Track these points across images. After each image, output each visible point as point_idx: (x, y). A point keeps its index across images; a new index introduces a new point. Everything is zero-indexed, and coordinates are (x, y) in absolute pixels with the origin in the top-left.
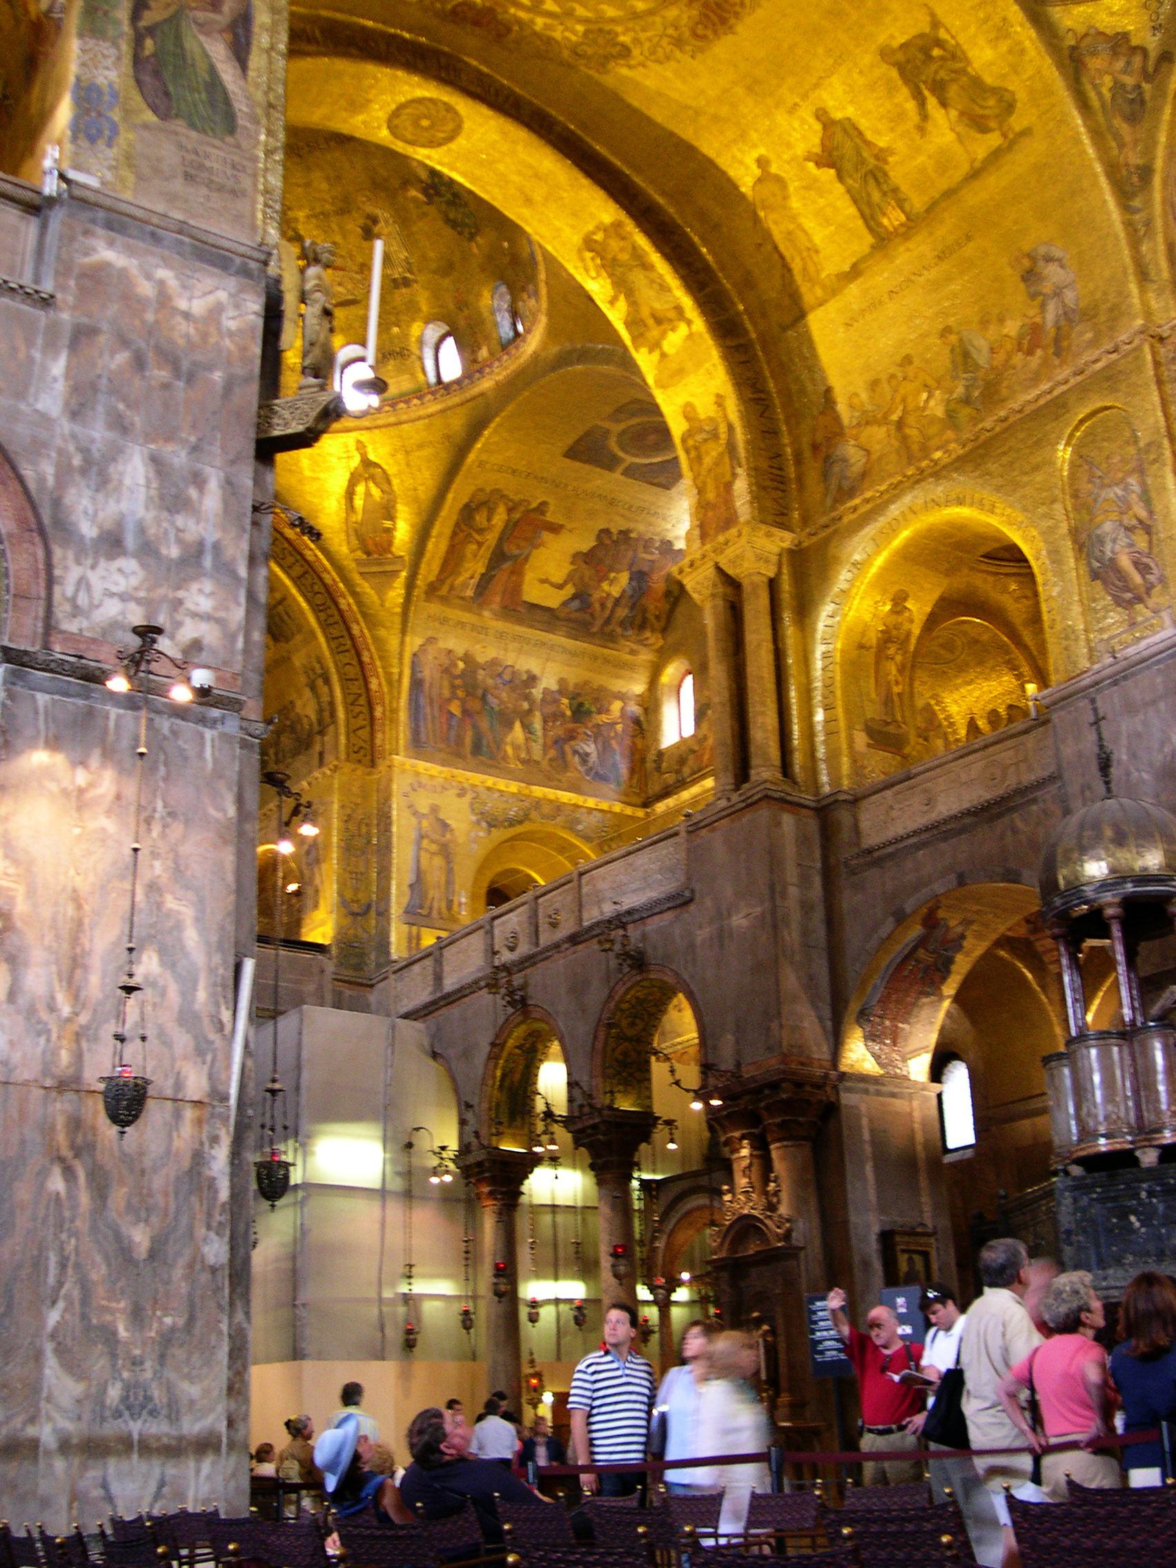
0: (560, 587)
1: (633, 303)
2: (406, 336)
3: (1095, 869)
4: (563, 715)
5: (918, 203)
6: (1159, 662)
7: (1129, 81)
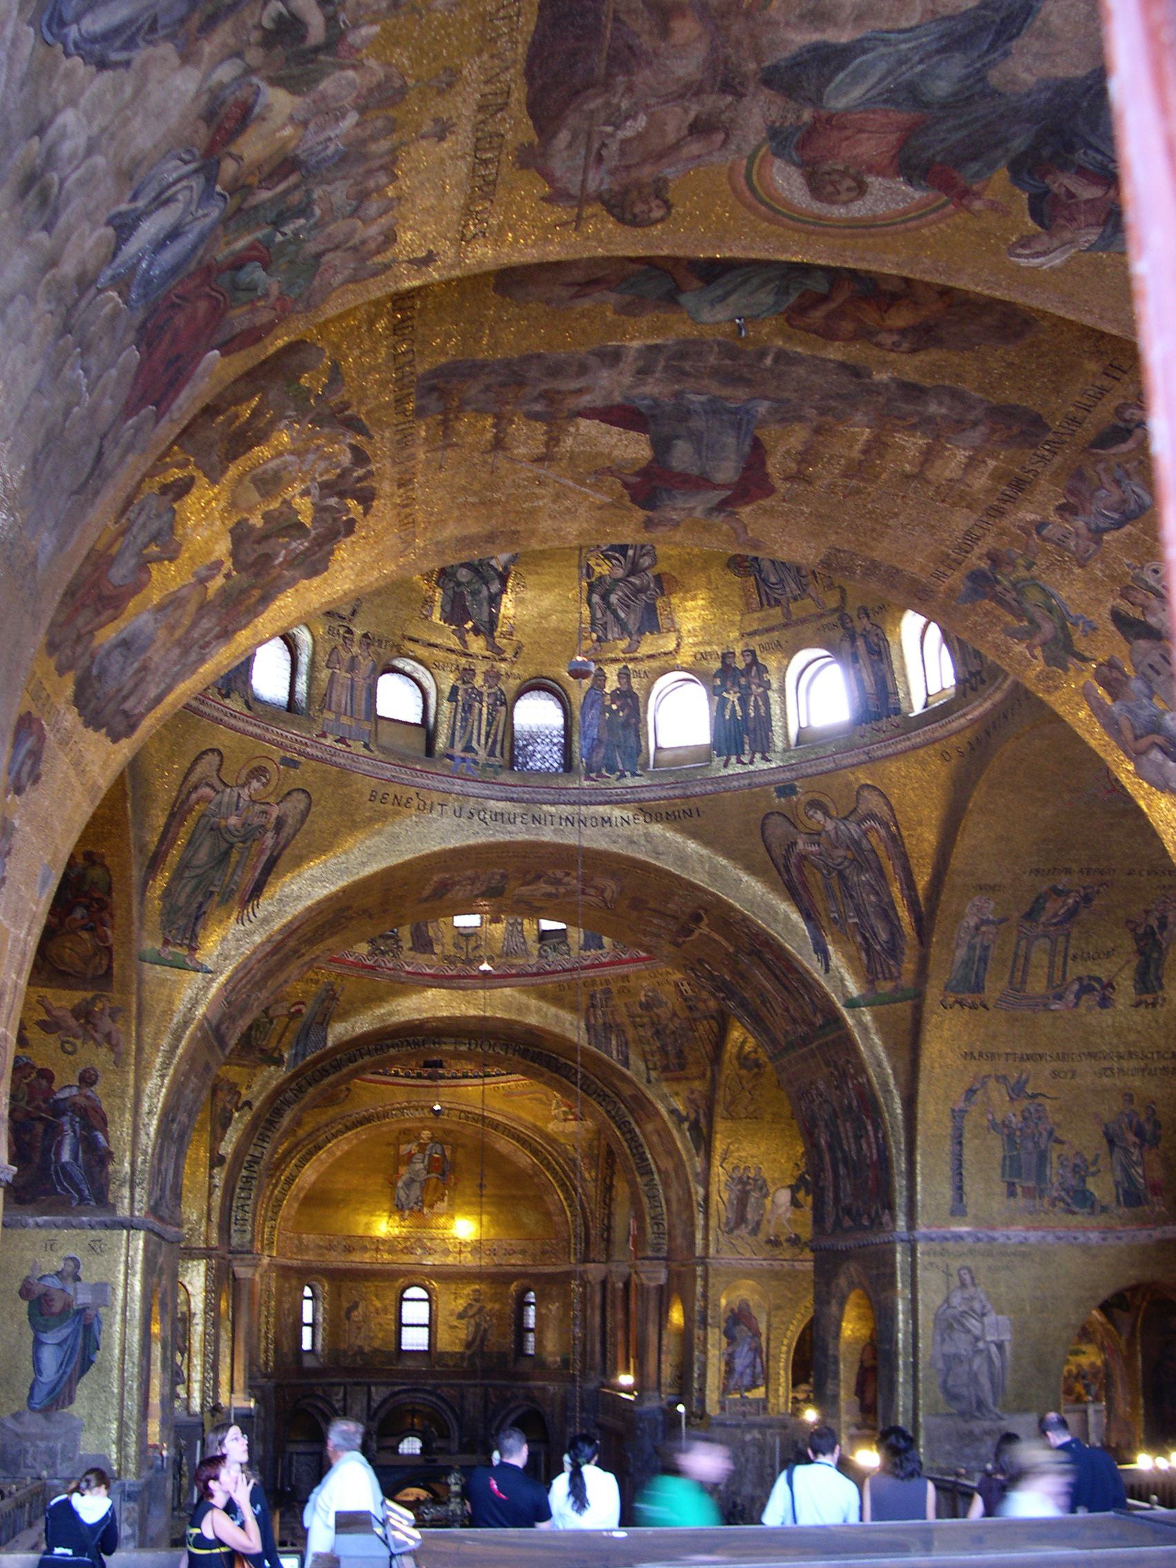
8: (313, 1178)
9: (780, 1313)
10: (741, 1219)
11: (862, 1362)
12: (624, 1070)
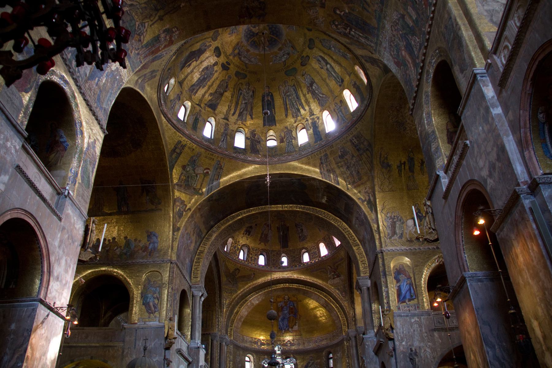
7: (182, 210)
8: (246, 313)
9: (418, 268)
10: (394, 233)
11: (448, 130)
12: (338, 186)
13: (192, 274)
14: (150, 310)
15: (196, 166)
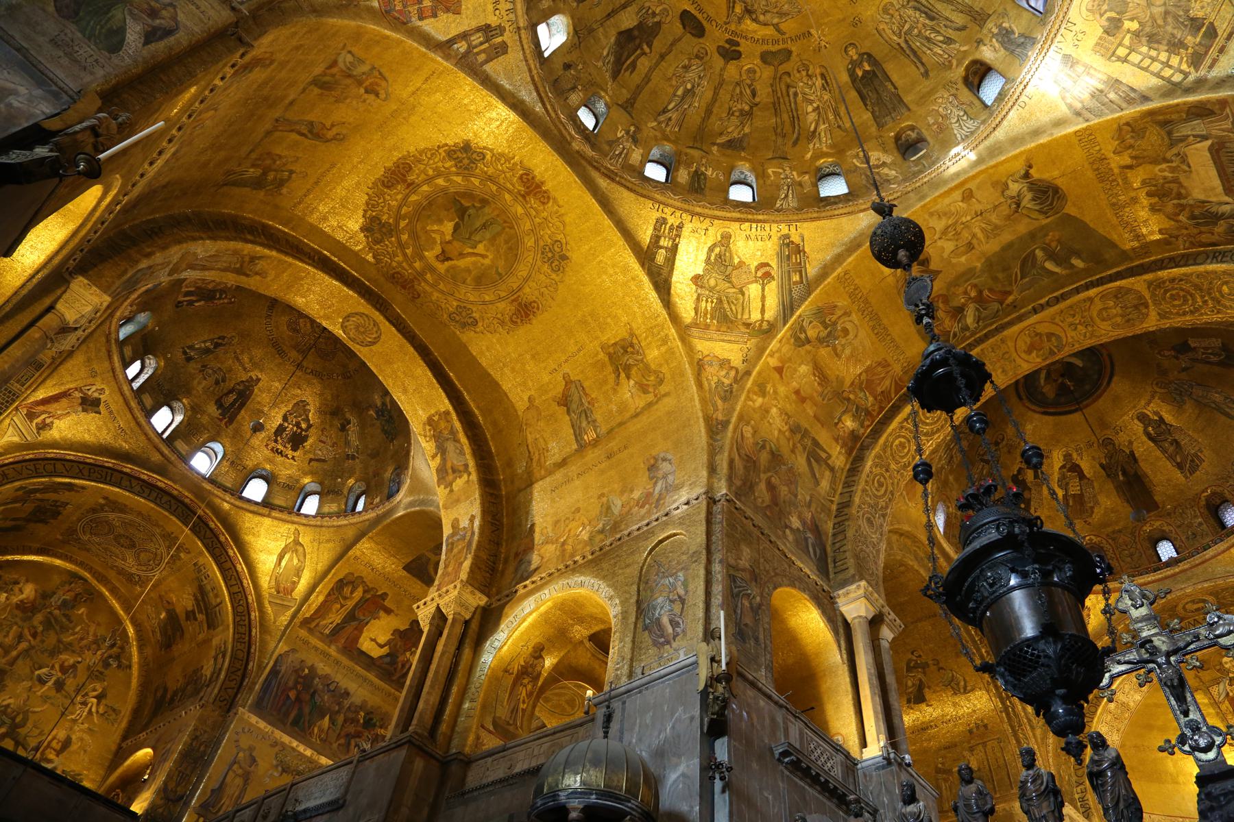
0: (381, 646)
1: (444, 460)
2: (344, 484)
3: (573, 781)
4: (358, 721)
5: (603, 429)
6: (669, 679)
7: (727, 382)
13: (831, 566)
14: (662, 636)
15: (730, 268)
